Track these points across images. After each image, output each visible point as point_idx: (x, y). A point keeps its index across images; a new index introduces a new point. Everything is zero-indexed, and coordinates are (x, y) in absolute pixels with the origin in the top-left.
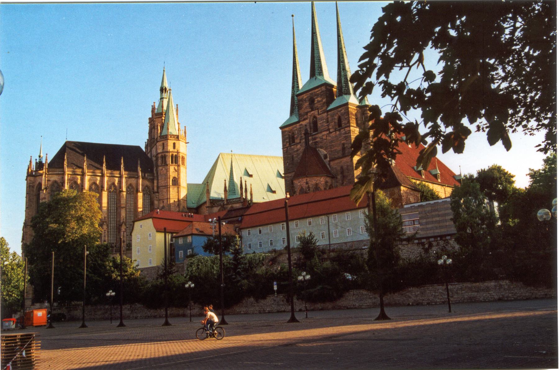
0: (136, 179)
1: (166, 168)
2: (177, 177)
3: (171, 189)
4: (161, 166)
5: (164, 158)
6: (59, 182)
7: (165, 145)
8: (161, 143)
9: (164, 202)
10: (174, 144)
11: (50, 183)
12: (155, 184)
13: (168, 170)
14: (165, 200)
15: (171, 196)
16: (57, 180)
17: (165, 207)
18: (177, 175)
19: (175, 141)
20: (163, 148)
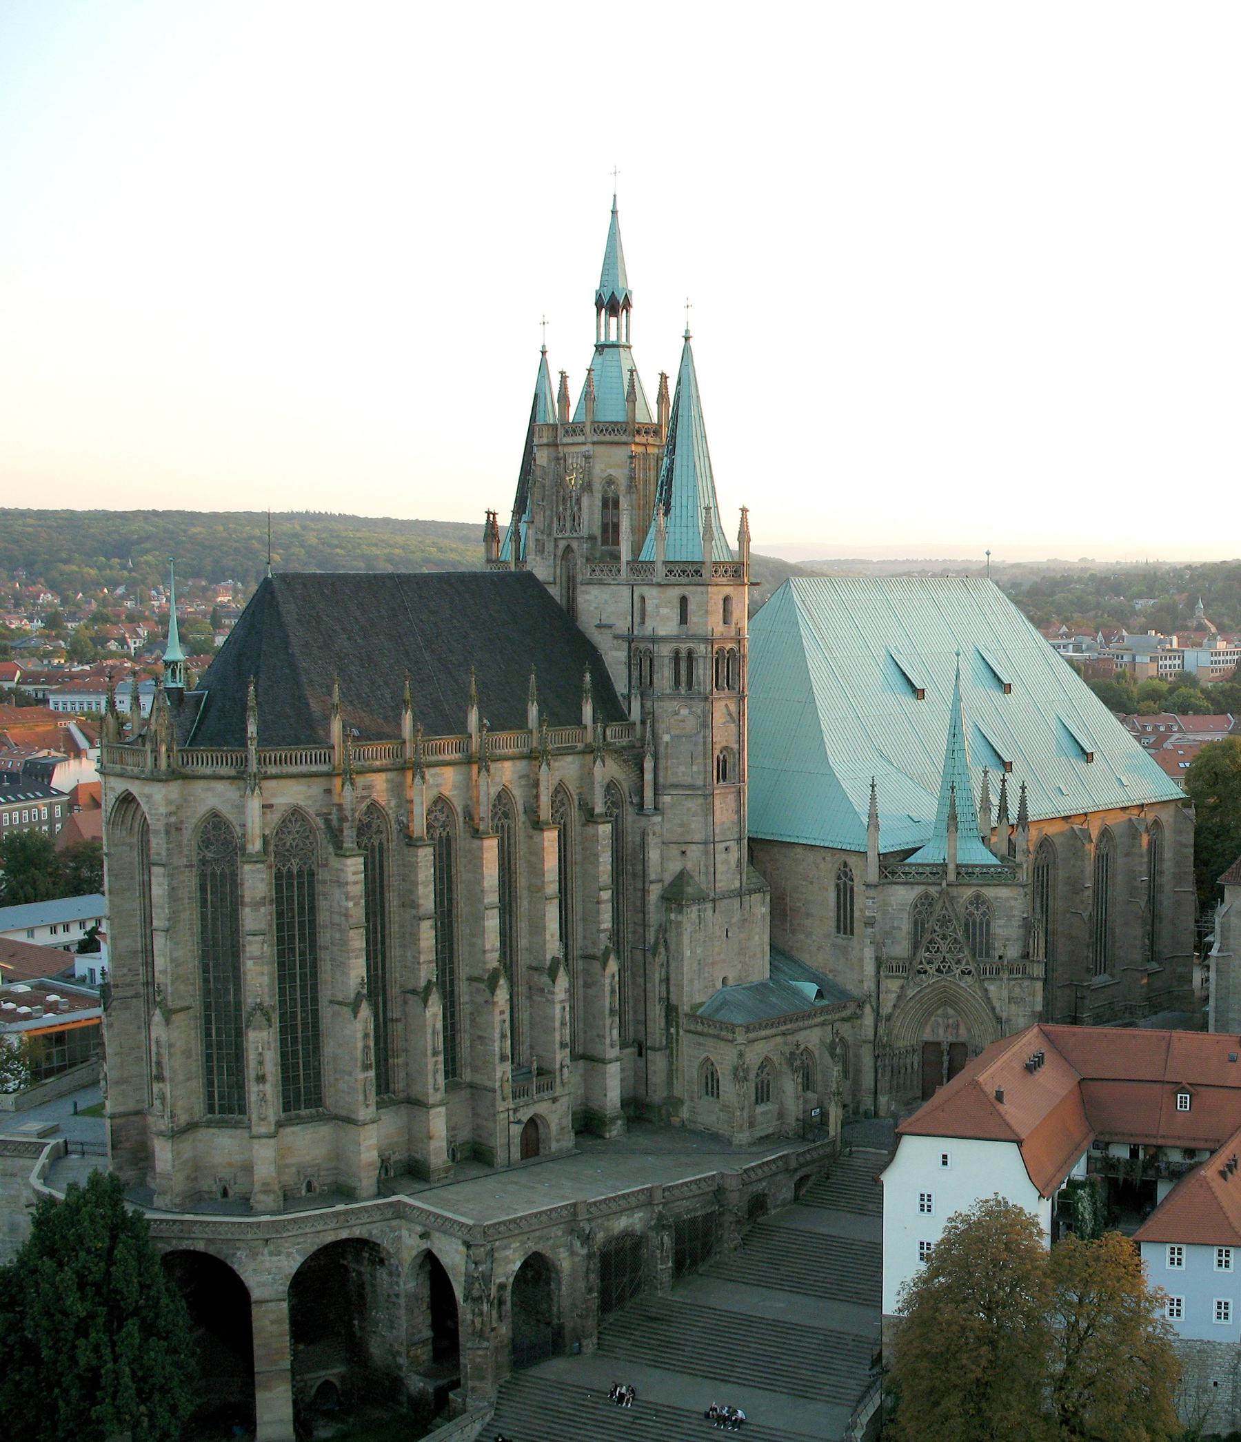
0: (576, 757)
1: (699, 711)
2: (736, 746)
3: (717, 802)
4: (671, 697)
5: (684, 662)
6: (312, 812)
7: (691, 607)
8: (676, 592)
9: (688, 853)
10: (726, 600)
11: (275, 817)
12: (648, 776)
13: (706, 722)
14: (694, 847)
16: (302, 803)
17: (695, 874)
18: (735, 738)
19: (728, 590)
20: (683, 619)
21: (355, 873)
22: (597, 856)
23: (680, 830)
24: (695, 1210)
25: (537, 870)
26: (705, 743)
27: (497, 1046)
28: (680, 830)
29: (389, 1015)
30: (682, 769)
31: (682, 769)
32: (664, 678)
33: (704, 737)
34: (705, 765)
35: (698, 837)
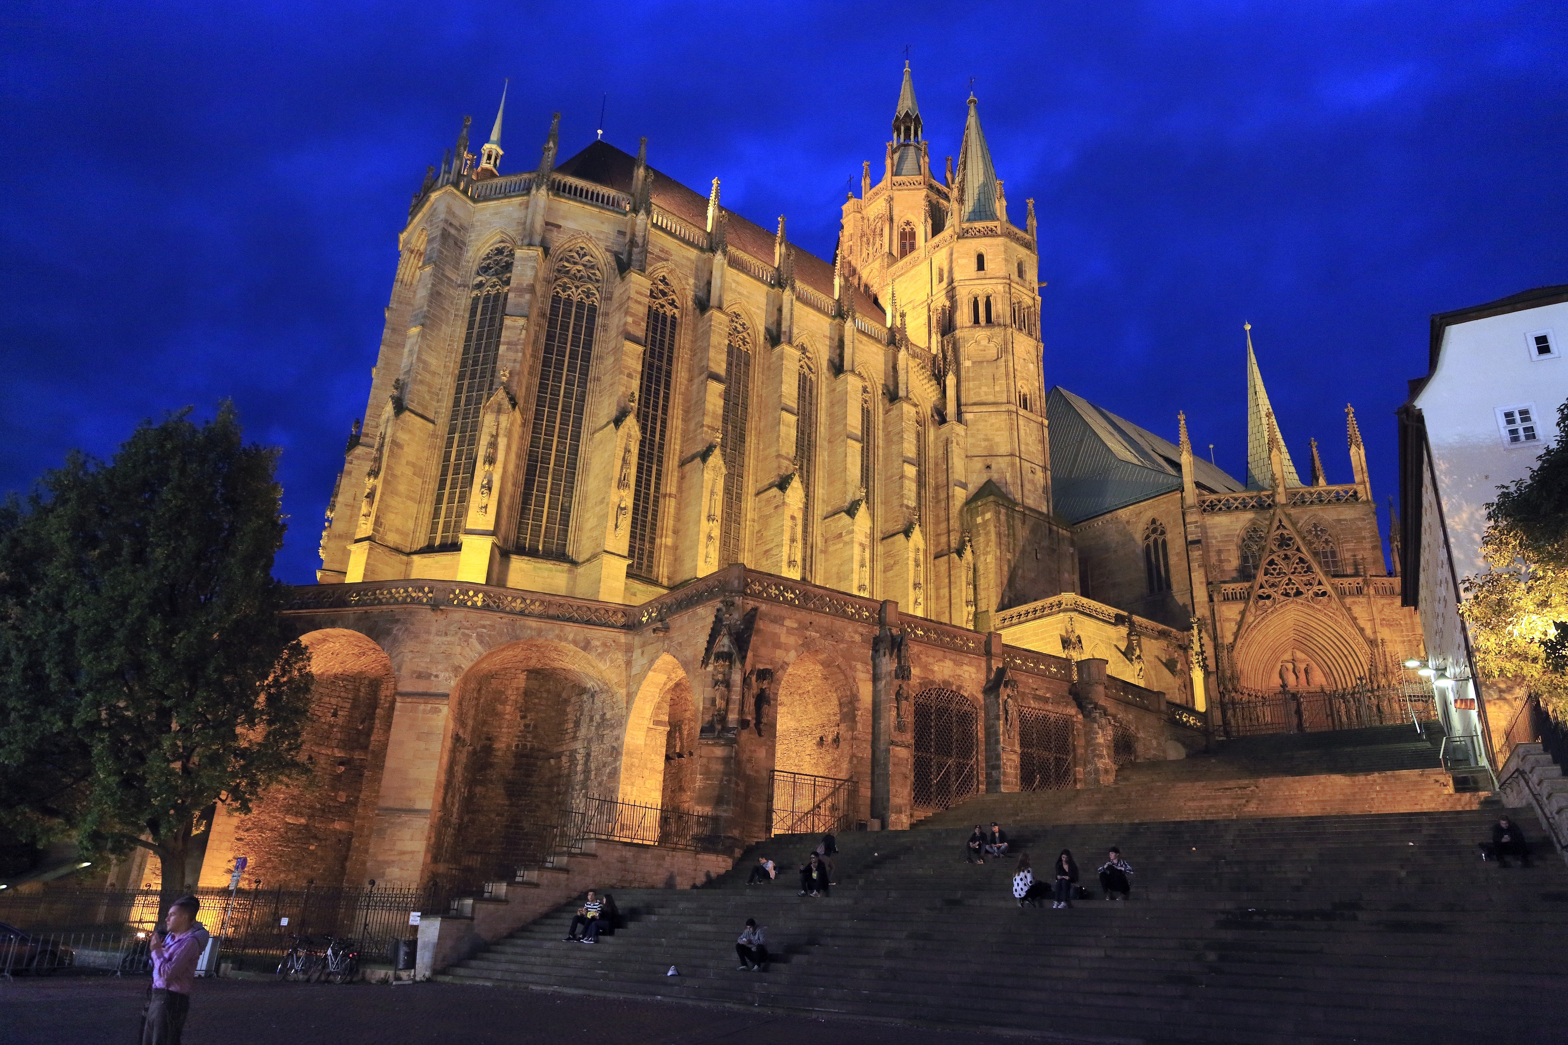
9: (994, 467)
12: (951, 392)
15: (1023, 448)
21: (638, 293)
22: (901, 433)
23: (984, 444)
24: (1046, 700)
25: (838, 418)
26: (1007, 366)
27: (786, 549)
28: (984, 444)
29: (662, 490)
30: (984, 389)
31: (984, 389)
32: (964, 316)
33: (1006, 361)
34: (1008, 385)
35: (1004, 449)
